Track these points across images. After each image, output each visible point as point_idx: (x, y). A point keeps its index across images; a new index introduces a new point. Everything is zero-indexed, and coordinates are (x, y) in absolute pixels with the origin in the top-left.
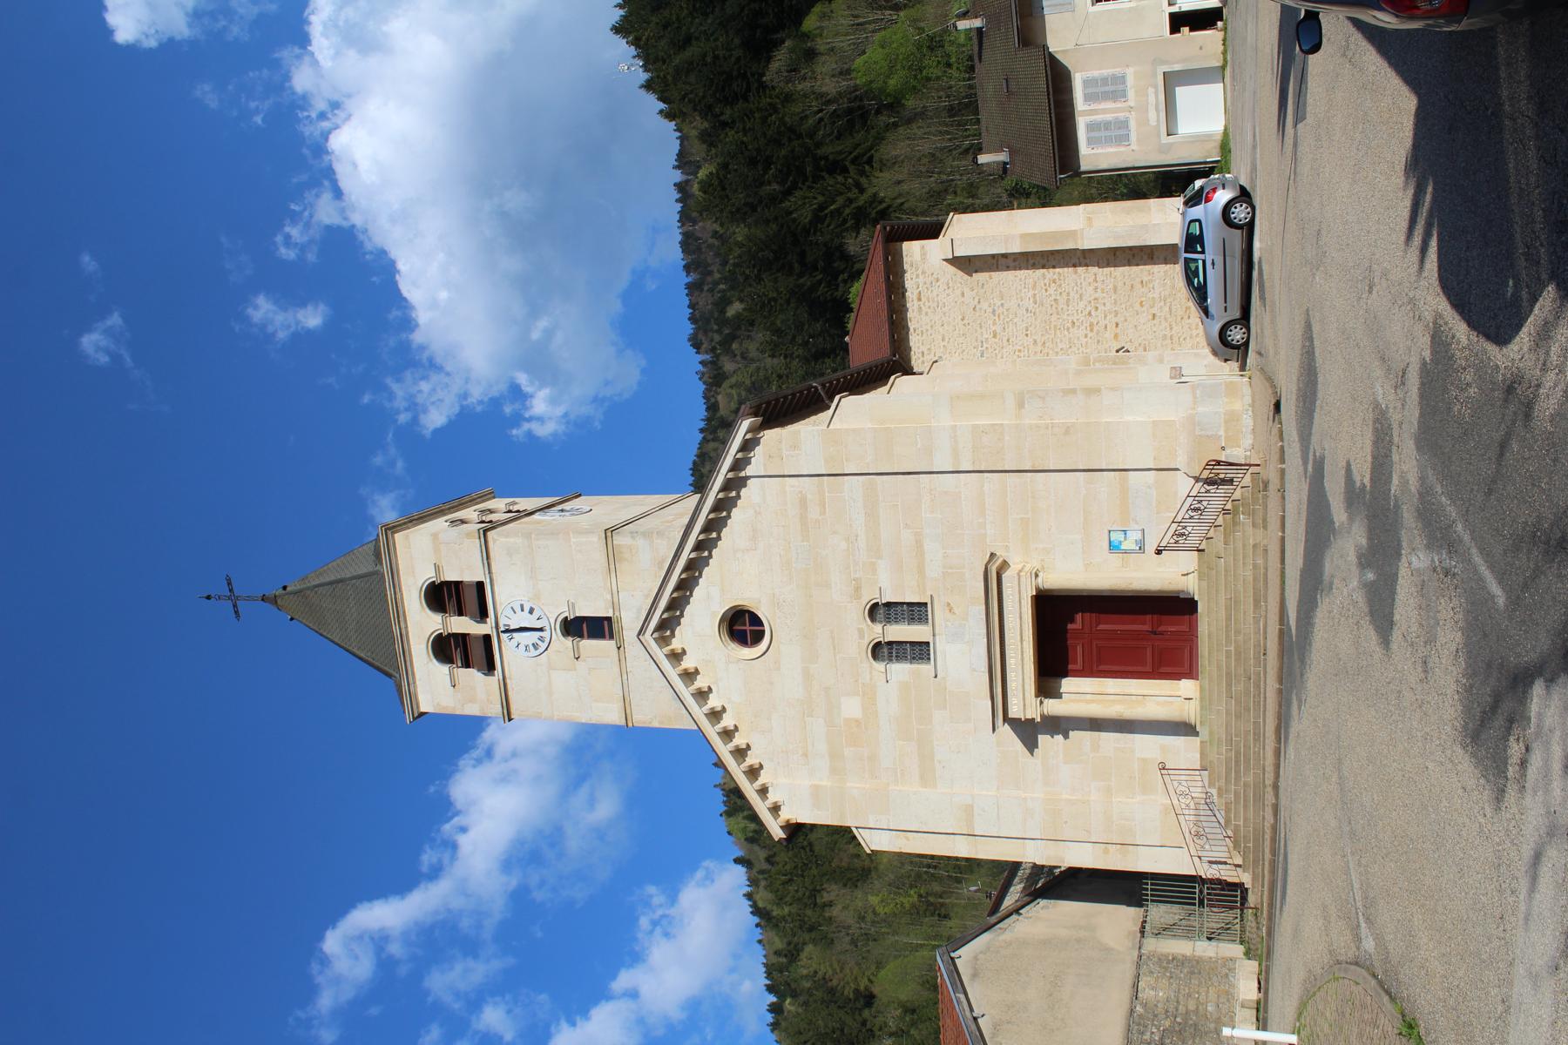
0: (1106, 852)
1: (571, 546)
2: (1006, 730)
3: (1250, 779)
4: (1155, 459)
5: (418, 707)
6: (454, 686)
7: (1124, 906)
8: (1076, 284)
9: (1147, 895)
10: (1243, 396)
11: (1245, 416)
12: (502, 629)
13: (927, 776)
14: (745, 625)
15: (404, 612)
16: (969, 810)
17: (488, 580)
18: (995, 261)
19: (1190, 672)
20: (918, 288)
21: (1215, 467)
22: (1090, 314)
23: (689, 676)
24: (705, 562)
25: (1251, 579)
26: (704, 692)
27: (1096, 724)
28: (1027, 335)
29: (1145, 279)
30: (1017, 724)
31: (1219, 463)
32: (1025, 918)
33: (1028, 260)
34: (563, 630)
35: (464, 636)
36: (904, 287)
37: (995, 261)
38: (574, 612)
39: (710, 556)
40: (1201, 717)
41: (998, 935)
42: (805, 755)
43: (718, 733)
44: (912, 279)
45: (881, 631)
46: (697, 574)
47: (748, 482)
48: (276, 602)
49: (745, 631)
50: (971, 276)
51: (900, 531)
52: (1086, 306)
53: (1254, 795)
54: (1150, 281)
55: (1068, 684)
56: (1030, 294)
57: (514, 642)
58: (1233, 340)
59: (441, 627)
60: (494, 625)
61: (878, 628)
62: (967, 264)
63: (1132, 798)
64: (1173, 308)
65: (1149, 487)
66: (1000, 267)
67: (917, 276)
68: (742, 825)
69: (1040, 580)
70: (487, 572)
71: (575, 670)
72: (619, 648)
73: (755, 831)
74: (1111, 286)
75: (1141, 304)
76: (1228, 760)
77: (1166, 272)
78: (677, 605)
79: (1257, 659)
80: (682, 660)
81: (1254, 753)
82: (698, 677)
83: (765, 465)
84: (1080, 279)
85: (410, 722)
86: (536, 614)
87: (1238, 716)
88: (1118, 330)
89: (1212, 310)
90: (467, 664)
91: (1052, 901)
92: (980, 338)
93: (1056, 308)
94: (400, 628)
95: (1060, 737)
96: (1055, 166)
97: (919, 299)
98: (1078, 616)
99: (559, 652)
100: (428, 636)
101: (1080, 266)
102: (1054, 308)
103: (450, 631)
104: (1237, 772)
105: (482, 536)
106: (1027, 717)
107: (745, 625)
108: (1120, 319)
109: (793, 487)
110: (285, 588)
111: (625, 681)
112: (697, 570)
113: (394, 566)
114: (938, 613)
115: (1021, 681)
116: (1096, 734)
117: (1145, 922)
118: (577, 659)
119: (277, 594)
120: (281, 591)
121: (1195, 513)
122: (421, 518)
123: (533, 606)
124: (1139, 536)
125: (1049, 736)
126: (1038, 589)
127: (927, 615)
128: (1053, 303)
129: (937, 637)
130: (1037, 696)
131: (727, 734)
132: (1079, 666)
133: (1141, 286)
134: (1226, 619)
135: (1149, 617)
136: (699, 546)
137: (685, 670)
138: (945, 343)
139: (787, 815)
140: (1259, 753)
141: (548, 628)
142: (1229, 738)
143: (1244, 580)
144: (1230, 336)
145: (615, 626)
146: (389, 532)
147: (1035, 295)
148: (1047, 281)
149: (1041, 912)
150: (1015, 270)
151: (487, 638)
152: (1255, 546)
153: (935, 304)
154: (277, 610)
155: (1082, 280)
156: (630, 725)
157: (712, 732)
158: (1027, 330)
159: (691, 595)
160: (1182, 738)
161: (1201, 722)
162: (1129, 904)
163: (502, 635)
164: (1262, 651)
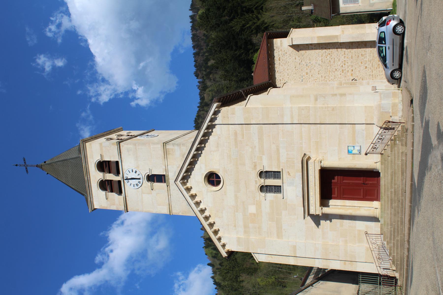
0: (345, 264)
1: (150, 149)
2: (309, 218)
3: (399, 238)
4: (365, 120)
5: (94, 206)
6: (107, 199)
7: (351, 284)
8: (338, 55)
9: (360, 280)
10: (399, 97)
11: (399, 105)
12: (125, 178)
13: (279, 235)
14: (214, 179)
16: (294, 248)
17: (120, 161)
18: (307, 46)
19: (377, 198)
20: (279, 56)
21: (388, 123)
22: (342, 66)
23: (193, 197)
24: (200, 155)
25: (401, 165)
26: (199, 202)
27: (342, 217)
28: (319, 74)
29: (363, 54)
30: (314, 217)
31: (389, 122)
32: (315, 288)
33: (320, 46)
34: (147, 179)
35: (111, 181)
36: (274, 55)
37: (307, 46)
38: (151, 173)
39: (202, 153)
40: (381, 215)
41: (305, 294)
42: (235, 226)
43: (203, 218)
44: (277, 52)
45: (263, 182)
46: (196, 160)
47: (216, 126)
48: (42, 167)
49: (214, 180)
50: (299, 52)
51: (271, 145)
52: (341, 63)
53: (400, 245)
54: (365, 54)
55: (332, 202)
56: (320, 59)
57: (129, 183)
58: (395, 77)
59: (103, 177)
60: (122, 177)
61: (262, 180)
62: (297, 47)
63: (355, 244)
64: (373, 64)
65: (363, 130)
66: (309, 49)
67: (279, 52)
69: (322, 164)
70: (120, 158)
71: (151, 194)
72: (168, 186)
73: (215, 254)
74: (350, 56)
75: (361, 63)
76: (391, 231)
77: (371, 51)
78: (189, 170)
79: (402, 194)
80: (191, 191)
81: (401, 229)
82: (196, 197)
83: (222, 120)
84: (339, 53)
85: (91, 212)
86: (138, 173)
87: (395, 215)
88: (353, 72)
89: (388, 65)
90: (112, 191)
91: (325, 282)
92: (301, 75)
93: (330, 64)
94: (87, 178)
95: (328, 222)
96: (331, 11)
97: (279, 60)
98: (336, 177)
99: (146, 187)
100: (97, 181)
101: (339, 48)
102: (329, 64)
103: (106, 179)
104: (394, 236)
105: (118, 144)
106: (316, 214)
107: (214, 179)
108: (353, 68)
109: (232, 128)
110: (45, 162)
111: (170, 198)
112: (196, 158)
113: (86, 155)
114: (285, 175)
115: (314, 201)
116: (343, 220)
117: (359, 290)
118: (152, 190)
119: (42, 164)
120: (44, 163)
121: (380, 140)
122: (95, 137)
123: (137, 170)
124: (359, 148)
125: (324, 221)
126: (321, 167)
127: (280, 176)
128: (329, 62)
129: (284, 184)
130: (320, 206)
131: (207, 218)
132: (336, 196)
134: (391, 179)
135: (362, 178)
136: (197, 149)
137: (192, 194)
138: (289, 76)
139: (228, 248)
140: (402, 229)
141: (142, 178)
142: (391, 223)
143: (398, 165)
144: (394, 75)
145: (166, 178)
146: (84, 143)
147: (322, 59)
148: (327, 54)
149: (321, 285)
150: (315, 49)
151: (119, 182)
152: (402, 153)
153: (285, 62)
154: (42, 170)
155: (340, 54)
156: (171, 214)
157: (201, 217)
158: (319, 72)
159: (194, 167)
160: (374, 223)
161: (381, 217)
162: (353, 284)
163: (125, 180)
164: (404, 191)
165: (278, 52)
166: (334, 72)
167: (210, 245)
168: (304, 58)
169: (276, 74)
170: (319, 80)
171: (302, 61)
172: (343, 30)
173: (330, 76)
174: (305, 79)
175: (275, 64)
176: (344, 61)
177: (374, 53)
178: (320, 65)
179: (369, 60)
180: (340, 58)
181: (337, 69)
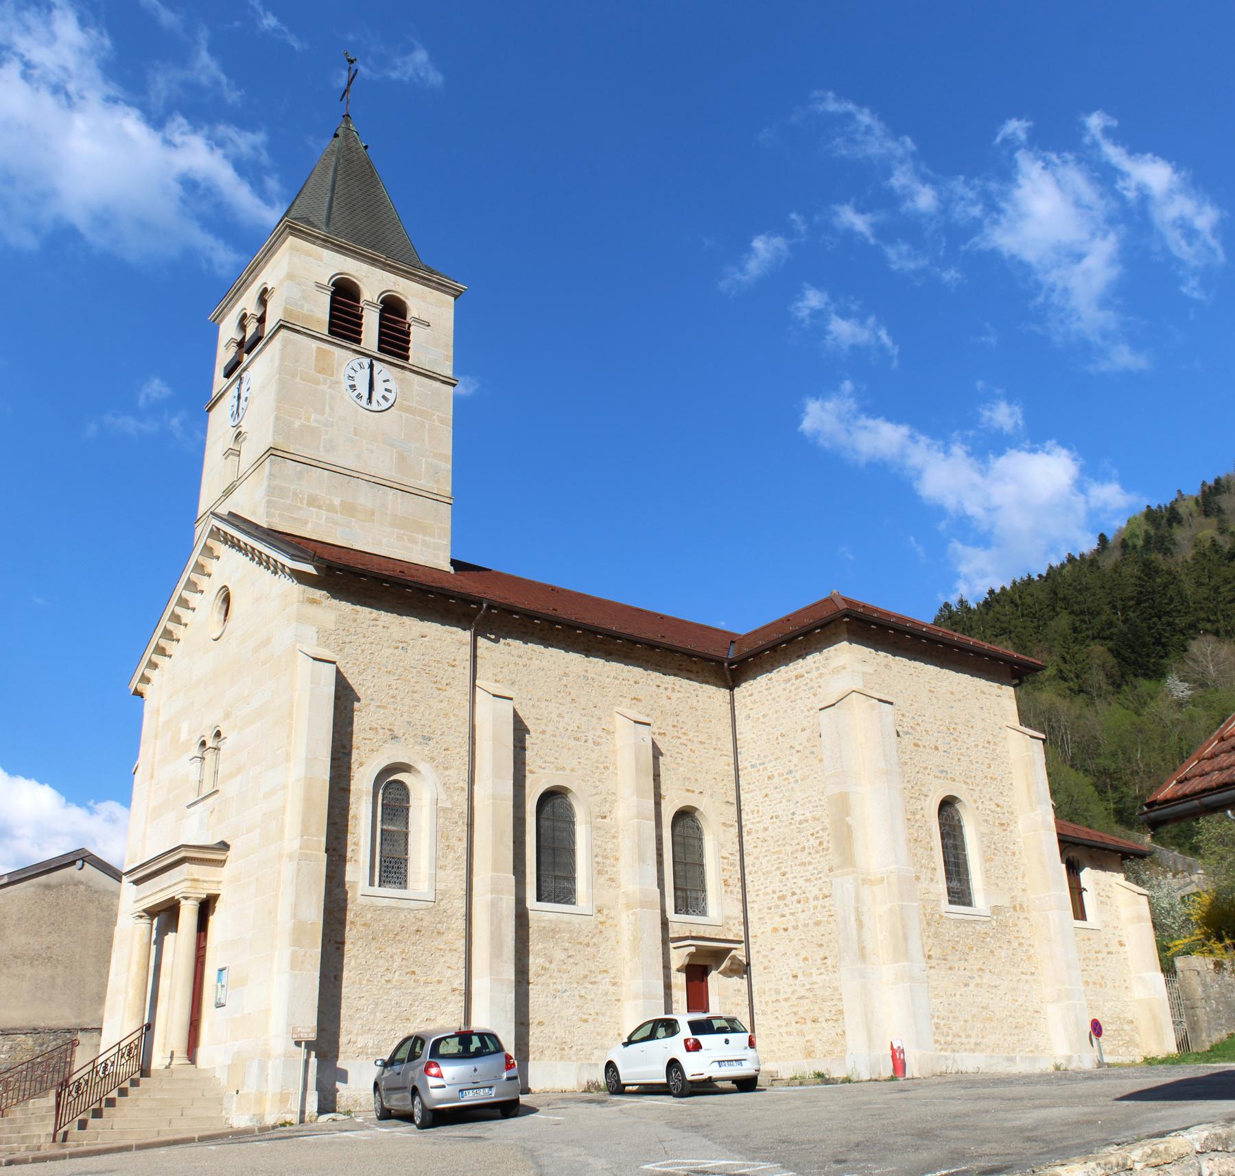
15: (257, 276)
20: (807, 673)
22: (794, 894)
28: (772, 818)
29: (828, 961)
36: (807, 654)
52: (801, 887)
56: (808, 815)
67: (818, 668)
68: (1138, 532)
73: (1134, 547)
75: (806, 959)
88: (781, 932)
92: (767, 760)
93: (797, 851)
94: (248, 278)
97: (797, 677)
102: (798, 847)
108: (791, 931)
128: (802, 845)
133: (821, 956)
138: (761, 719)
146: (288, 230)
158: (777, 817)
165: (817, 665)
166: (778, 868)
167: (1160, 524)
168: (807, 757)
169: (764, 676)
170: (758, 822)
171: (800, 754)
172: (885, 881)
173: (768, 858)
174: (757, 774)
175: (787, 665)
176: (807, 898)
177: (832, 1000)
178: (792, 819)
179: (812, 986)
180: (813, 884)
181: (787, 876)
